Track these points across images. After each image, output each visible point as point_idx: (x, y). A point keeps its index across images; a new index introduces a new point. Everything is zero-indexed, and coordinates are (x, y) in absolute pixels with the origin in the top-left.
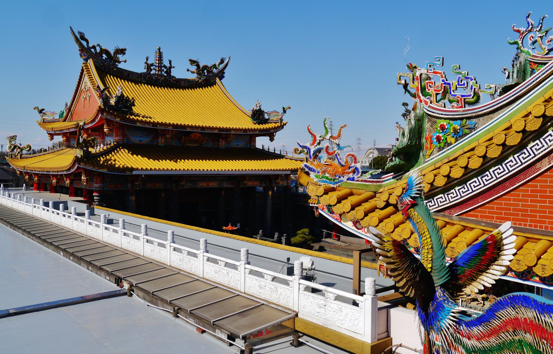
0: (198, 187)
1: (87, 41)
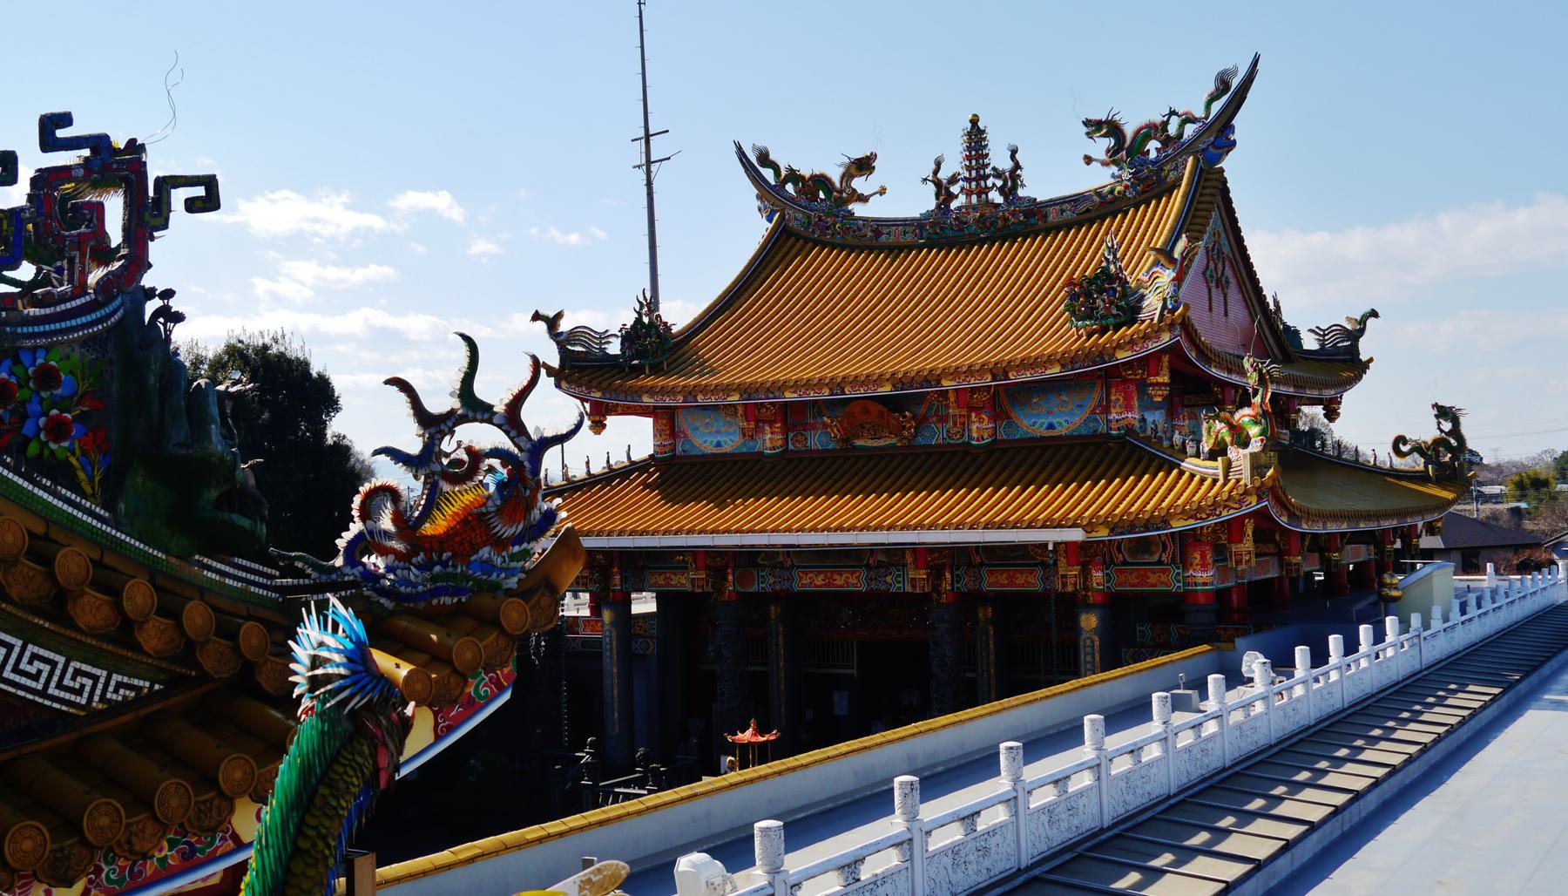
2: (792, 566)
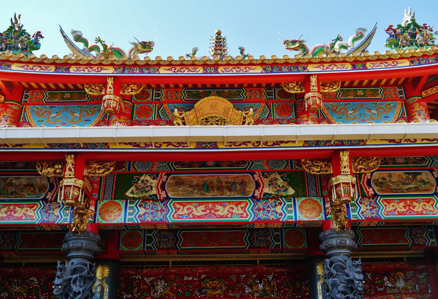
1: (86, 42)
2: (168, 198)
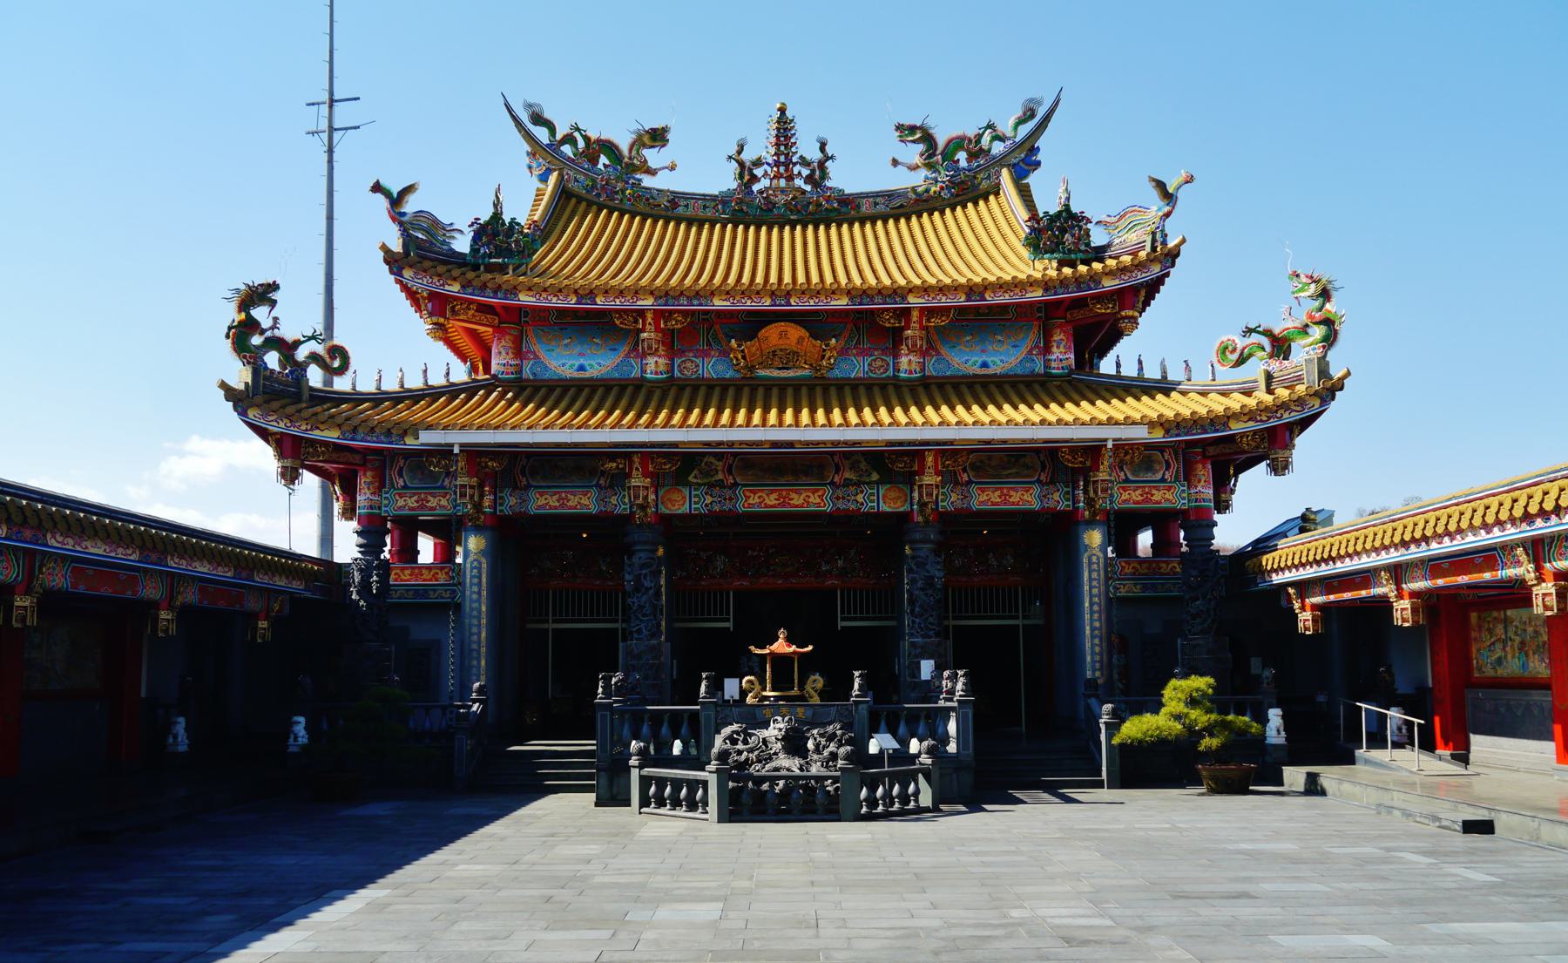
0: (741, 507)
2: (736, 485)
